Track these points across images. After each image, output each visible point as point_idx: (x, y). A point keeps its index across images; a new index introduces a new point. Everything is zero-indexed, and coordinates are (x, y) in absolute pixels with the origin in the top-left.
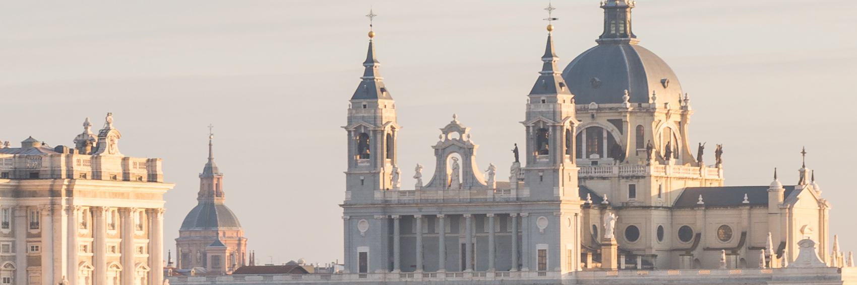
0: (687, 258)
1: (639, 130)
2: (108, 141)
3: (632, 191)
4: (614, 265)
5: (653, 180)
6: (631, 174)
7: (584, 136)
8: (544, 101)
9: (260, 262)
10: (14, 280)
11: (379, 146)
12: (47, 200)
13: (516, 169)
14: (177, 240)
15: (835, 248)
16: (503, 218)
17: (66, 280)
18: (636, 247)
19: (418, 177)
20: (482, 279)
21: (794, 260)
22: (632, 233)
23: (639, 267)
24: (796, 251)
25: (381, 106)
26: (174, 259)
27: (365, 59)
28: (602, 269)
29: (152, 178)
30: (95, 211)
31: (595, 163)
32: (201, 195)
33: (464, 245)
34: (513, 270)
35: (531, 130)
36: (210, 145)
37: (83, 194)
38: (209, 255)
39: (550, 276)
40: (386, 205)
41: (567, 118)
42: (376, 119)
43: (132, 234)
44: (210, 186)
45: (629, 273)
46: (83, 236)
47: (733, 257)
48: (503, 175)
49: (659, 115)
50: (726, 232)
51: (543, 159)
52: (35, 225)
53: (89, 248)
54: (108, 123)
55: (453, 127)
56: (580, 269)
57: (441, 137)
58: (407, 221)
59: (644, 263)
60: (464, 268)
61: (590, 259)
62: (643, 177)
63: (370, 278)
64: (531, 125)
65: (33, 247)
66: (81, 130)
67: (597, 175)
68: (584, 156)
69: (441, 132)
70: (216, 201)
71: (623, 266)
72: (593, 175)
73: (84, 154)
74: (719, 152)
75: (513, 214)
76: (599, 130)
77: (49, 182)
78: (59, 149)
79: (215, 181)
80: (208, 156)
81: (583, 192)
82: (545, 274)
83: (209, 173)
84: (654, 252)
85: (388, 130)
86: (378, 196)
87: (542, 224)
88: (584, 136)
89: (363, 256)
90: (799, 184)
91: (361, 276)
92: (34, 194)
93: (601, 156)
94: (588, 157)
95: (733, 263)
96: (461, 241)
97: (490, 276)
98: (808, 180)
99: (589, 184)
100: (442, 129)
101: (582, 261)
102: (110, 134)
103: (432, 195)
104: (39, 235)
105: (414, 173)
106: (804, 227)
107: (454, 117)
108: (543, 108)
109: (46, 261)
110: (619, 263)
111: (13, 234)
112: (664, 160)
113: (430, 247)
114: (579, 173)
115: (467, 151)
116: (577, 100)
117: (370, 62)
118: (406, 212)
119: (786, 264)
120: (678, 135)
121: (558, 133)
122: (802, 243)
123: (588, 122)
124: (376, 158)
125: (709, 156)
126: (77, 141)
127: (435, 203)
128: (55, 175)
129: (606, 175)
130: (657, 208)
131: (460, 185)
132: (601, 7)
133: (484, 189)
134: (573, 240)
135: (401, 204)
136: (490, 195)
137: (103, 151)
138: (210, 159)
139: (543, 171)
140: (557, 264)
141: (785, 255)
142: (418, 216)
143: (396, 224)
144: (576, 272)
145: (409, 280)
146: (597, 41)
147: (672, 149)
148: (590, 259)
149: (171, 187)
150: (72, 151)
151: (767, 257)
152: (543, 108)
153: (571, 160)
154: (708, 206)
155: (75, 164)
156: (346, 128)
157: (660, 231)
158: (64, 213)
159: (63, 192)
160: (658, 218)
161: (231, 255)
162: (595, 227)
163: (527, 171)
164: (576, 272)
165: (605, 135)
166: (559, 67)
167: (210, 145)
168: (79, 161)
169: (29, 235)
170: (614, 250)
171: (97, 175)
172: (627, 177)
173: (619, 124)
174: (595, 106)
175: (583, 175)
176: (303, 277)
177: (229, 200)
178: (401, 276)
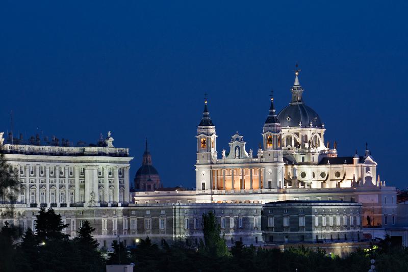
3: (303, 158)
8: (270, 126)
18: (305, 180)
22: (303, 175)
23: (306, 187)
24: (364, 181)
38: (147, 184)
44: (147, 159)
50: (338, 174)
52: (83, 173)
61: (287, 184)
70: (148, 164)
79: (149, 157)
81: (285, 159)
83: (146, 154)
93: (292, 146)
104: (84, 177)
148: (287, 184)
149: (132, 158)
154: (331, 164)
161: (155, 185)
165: (293, 138)
169: (80, 177)
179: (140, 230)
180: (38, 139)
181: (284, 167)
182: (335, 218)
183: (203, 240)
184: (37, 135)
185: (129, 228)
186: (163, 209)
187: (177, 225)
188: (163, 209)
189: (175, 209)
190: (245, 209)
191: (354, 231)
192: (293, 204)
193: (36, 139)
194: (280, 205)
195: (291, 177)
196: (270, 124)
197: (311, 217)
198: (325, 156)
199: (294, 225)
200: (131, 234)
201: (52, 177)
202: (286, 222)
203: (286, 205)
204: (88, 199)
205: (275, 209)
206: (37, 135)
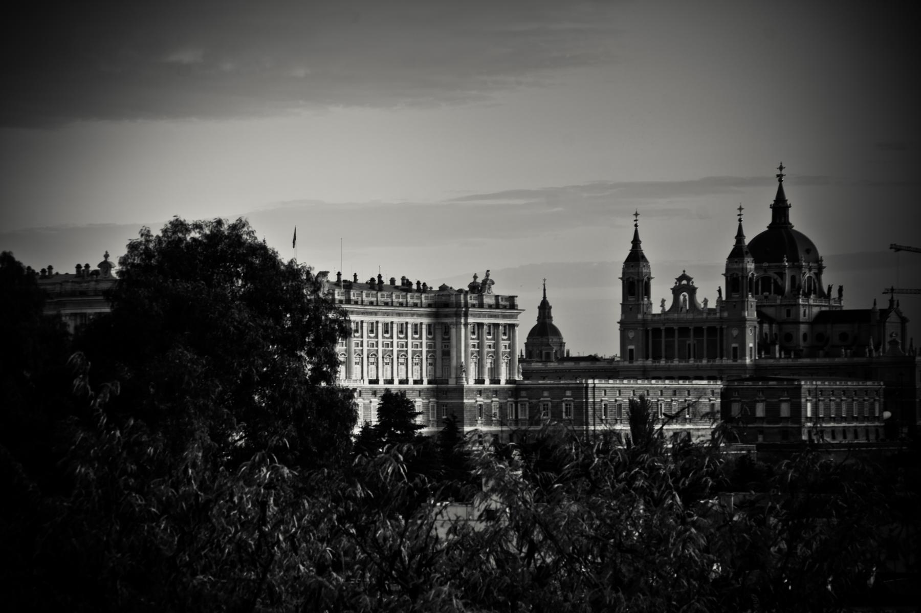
0: (821, 352)
1: (793, 279)
2: (487, 286)
4: (778, 355)
5: (801, 307)
6: (788, 303)
7: (760, 282)
8: (736, 262)
9: (573, 354)
10: (435, 363)
11: (641, 288)
12: (454, 320)
13: (718, 301)
14: (525, 343)
15: (911, 345)
16: (712, 331)
17: (464, 364)
19: (663, 306)
20: (700, 364)
21: (886, 351)
22: (789, 337)
23: (792, 356)
24: (888, 347)
25: (641, 266)
26: (524, 353)
27: (632, 239)
28: (771, 358)
29: (513, 306)
30: (480, 325)
31: (766, 297)
32: (539, 318)
33: (689, 345)
34: (718, 359)
35: (729, 278)
36: (545, 290)
37: (474, 316)
38: (544, 352)
39: (739, 361)
40: (644, 322)
41: (750, 271)
42: (639, 273)
43: (500, 339)
44: (544, 313)
45: (786, 360)
46: (473, 339)
47: (849, 351)
48: (712, 304)
49: (804, 270)
51: (736, 295)
53: (476, 346)
54: (487, 275)
55: (684, 277)
56: (757, 358)
57: (676, 283)
58: (656, 332)
59: (795, 354)
60: (689, 357)
61: (763, 353)
62: (795, 305)
63: (635, 364)
64: (728, 275)
65: (445, 346)
66: (472, 280)
67: (768, 304)
68: (760, 293)
69: (676, 281)
70: (547, 321)
71: (783, 356)
72: (765, 304)
73: (474, 293)
74: (840, 290)
75: (718, 327)
76: (769, 278)
77: (455, 310)
78: (460, 291)
79: (547, 311)
80: (542, 296)
82: (736, 361)
84: (801, 348)
85: (645, 278)
86: (640, 317)
87: (735, 332)
88: (760, 282)
89: (631, 350)
90: (890, 307)
91: (630, 362)
92: (447, 316)
93: (770, 293)
94: (762, 293)
95: (849, 354)
96: (688, 342)
97: (704, 362)
98: (895, 306)
99: (764, 310)
100: (677, 279)
101: (758, 354)
102: (488, 282)
103: (671, 316)
104: (449, 339)
105: (660, 304)
106: (893, 333)
107: (684, 271)
108: (736, 266)
109: (454, 354)
110: (780, 354)
111: (434, 339)
112: (807, 295)
113: (670, 346)
114: (757, 303)
115: (692, 291)
116: (756, 261)
117: (636, 242)
118: (656, 326)
119: (881, 354)
120: (816, 281)
121: (745, 281)
122: (890, 343)
123: (762, 273)
124: (638, 296)
125: (834, 294)
126: (470, 286)
127: (673, 321)
128: (458, 305)
129: (773, 304)
130: (803, 323)
131: (687, 311)
132: (771, 208)
133: (701, 312)
134: (753, 341)
135: (653, 321)
136: (705, 315)
137: (484, 292)
138: (545, 297)
139: (735, 302)
140: (743, 356)
141: (881, 350)
142: (663, 328)
143: (650, 333)
144: (755, 359)
145: (657, 364)
146: (768, 227)
147: (812, 288)
148: (763, 353)
150: (467, 292)
151: (870, 351)
152: (736, 266)
153: (753, 296)
155: (469, 299)
156: (621, 279)
157: (805, 335)
158: (462, 327)
159: (462, 315)
160: (803, 328)
161: (556, 351)
162: (766, 334)
163: (726, 301)
164: (755, 359)
165: (772, 281)
167: (545, 290)
168: (471, 297)
169: (443, 339)
170: (777, 347)
171: (481, 305)
172: (785, 305)
173: (782, 275)
174: (767, 265)
175: (759, 304)
176: (597, 363)
177: (557, 320)
178: (653, 362)
179: (534, 420)
180: (381, 282)
181: (757, 326)
182: (839, 405)
183: (630, 436)
184: (380, 277)
185: (517, 416)
186: (568, 389)
187: (590, 412)
188: (568, 389)
189: (587, 388)
190: (695, 389)
191: (869, 425)
192: (771, 383)
193: (377, 282)
194: (750, 383)
195: (768, 341)
196: (736, 260)
197: (800, 402)
198: (823, 309)
199: (773, 413)
200: (520, 425)
201: (401, 338)
202: (760, 411)
203: (760, 383)
204: (453, 376)
205: (742, 389)
206: (380, 277)
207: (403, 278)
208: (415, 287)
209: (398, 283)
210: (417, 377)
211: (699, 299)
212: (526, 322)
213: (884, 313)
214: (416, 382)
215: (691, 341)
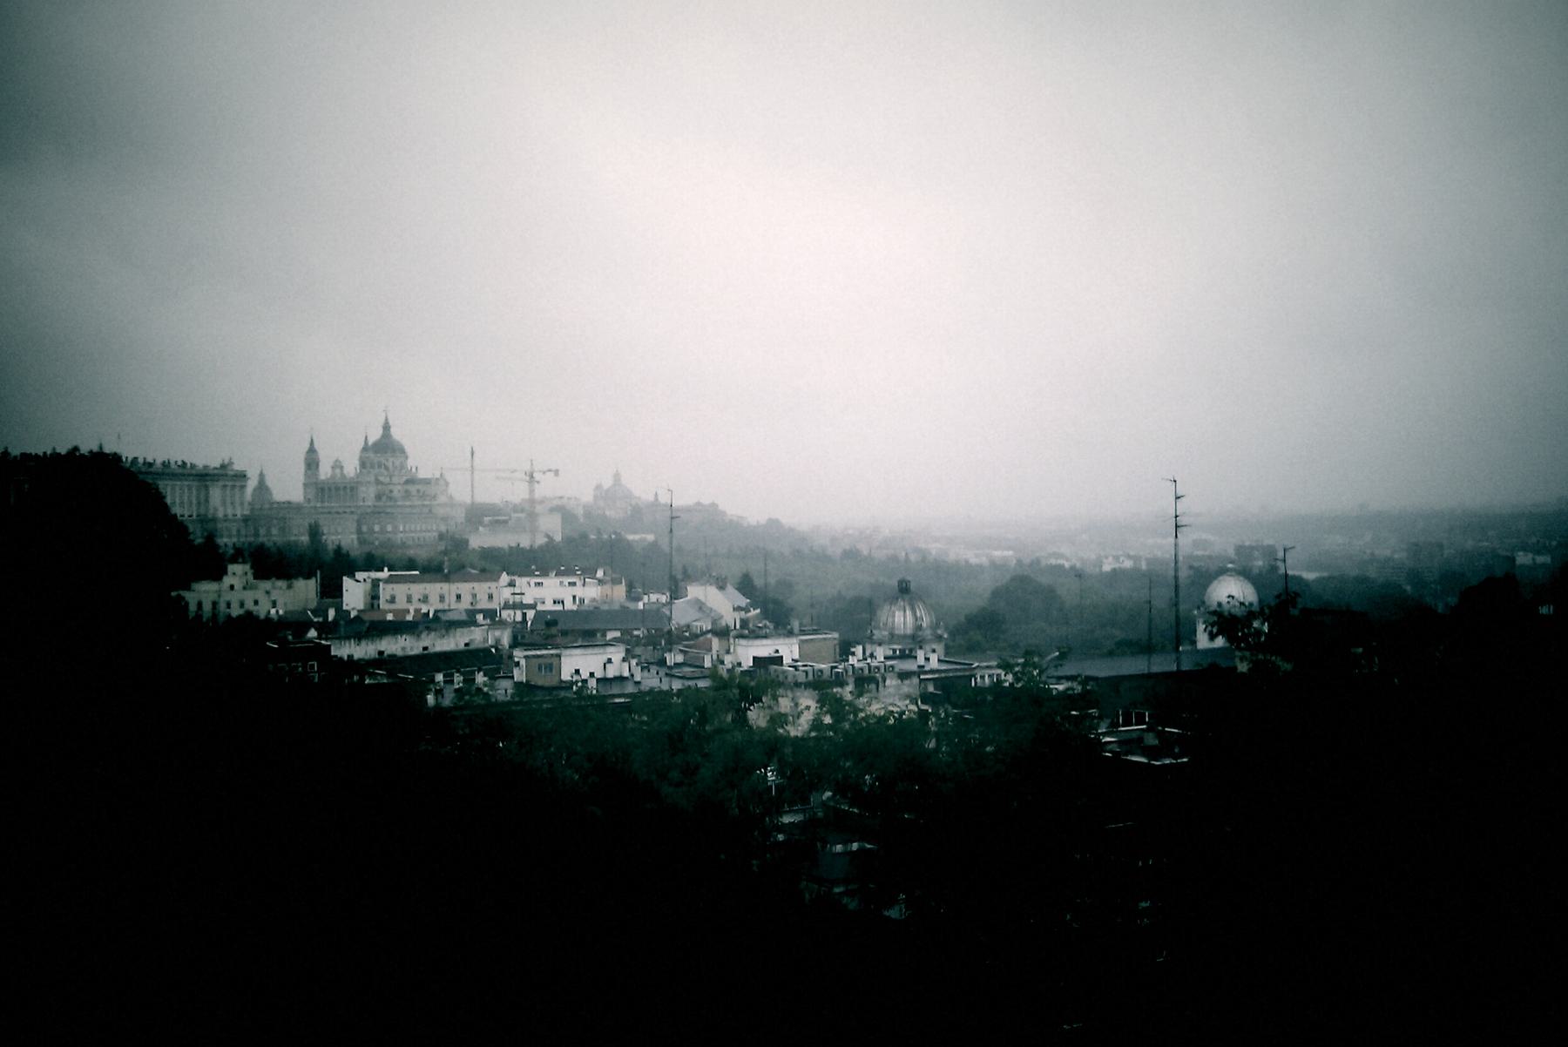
1: (393, 463)
16: (352, 489)
40: (316, 483)
50: (418, 491)
83: (262, 476)
86: (314, 480)
115: (342, 468)
117: (312, 443)
125: (414, 470)
166: (370, 443)
180: (169, 463)
199: (383, 531)
207: (183, 461)
208: (189, 465)
209: (180, 463)
210: (189, 513)
211: (345, 472)
212: (252, 484)
213: (437, 479)
214: (190, 516)
215: (342, 492)
